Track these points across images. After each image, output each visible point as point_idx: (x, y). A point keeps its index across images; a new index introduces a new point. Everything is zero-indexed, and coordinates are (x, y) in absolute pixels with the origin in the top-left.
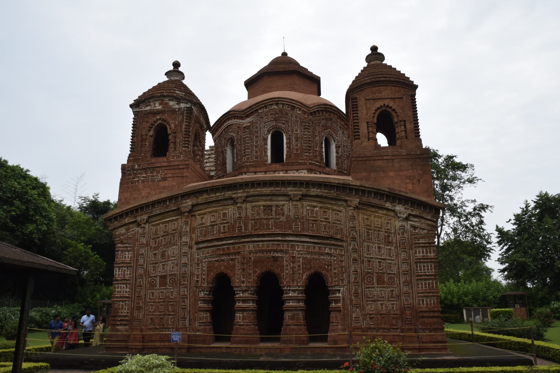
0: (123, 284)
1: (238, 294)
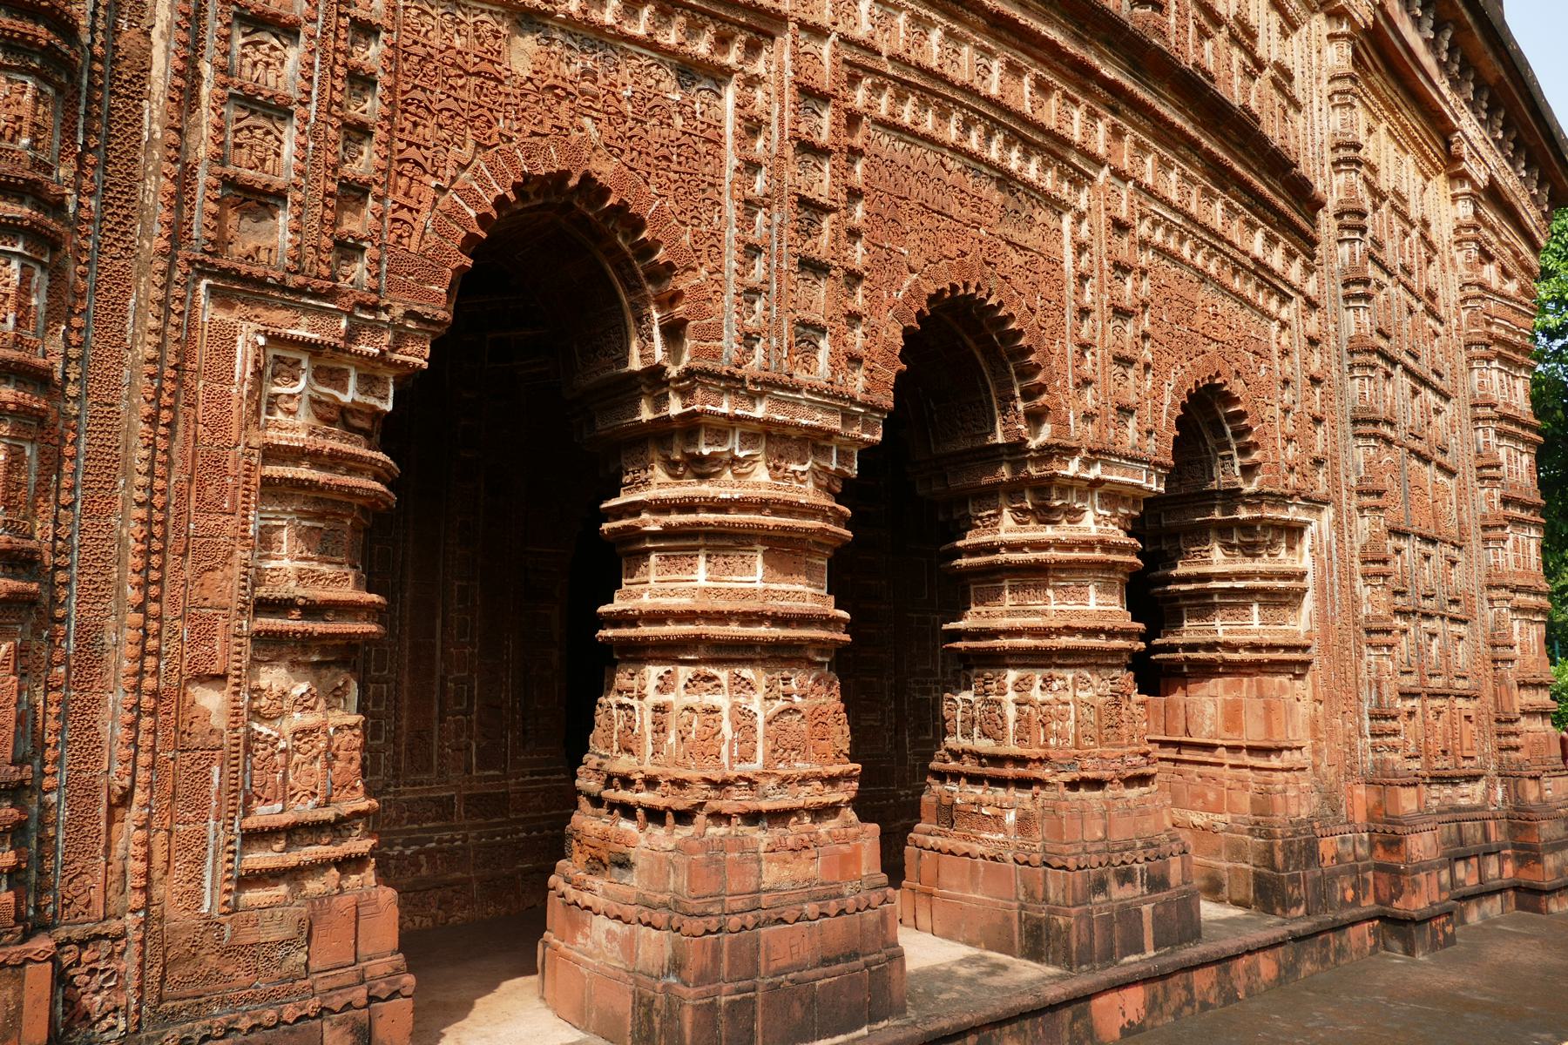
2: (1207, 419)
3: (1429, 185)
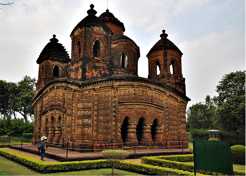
0: (87, 119)
1: (131, 126)
3: (176, 103)
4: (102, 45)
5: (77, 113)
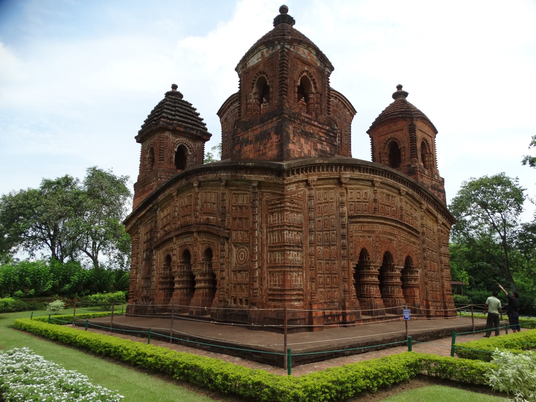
0: (295, 251)
2: (408, 260)
4: (313, 90)
5: (269, 237)
